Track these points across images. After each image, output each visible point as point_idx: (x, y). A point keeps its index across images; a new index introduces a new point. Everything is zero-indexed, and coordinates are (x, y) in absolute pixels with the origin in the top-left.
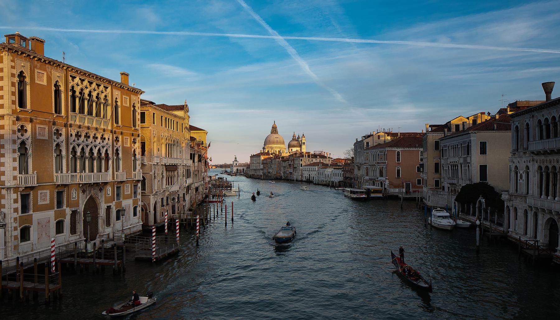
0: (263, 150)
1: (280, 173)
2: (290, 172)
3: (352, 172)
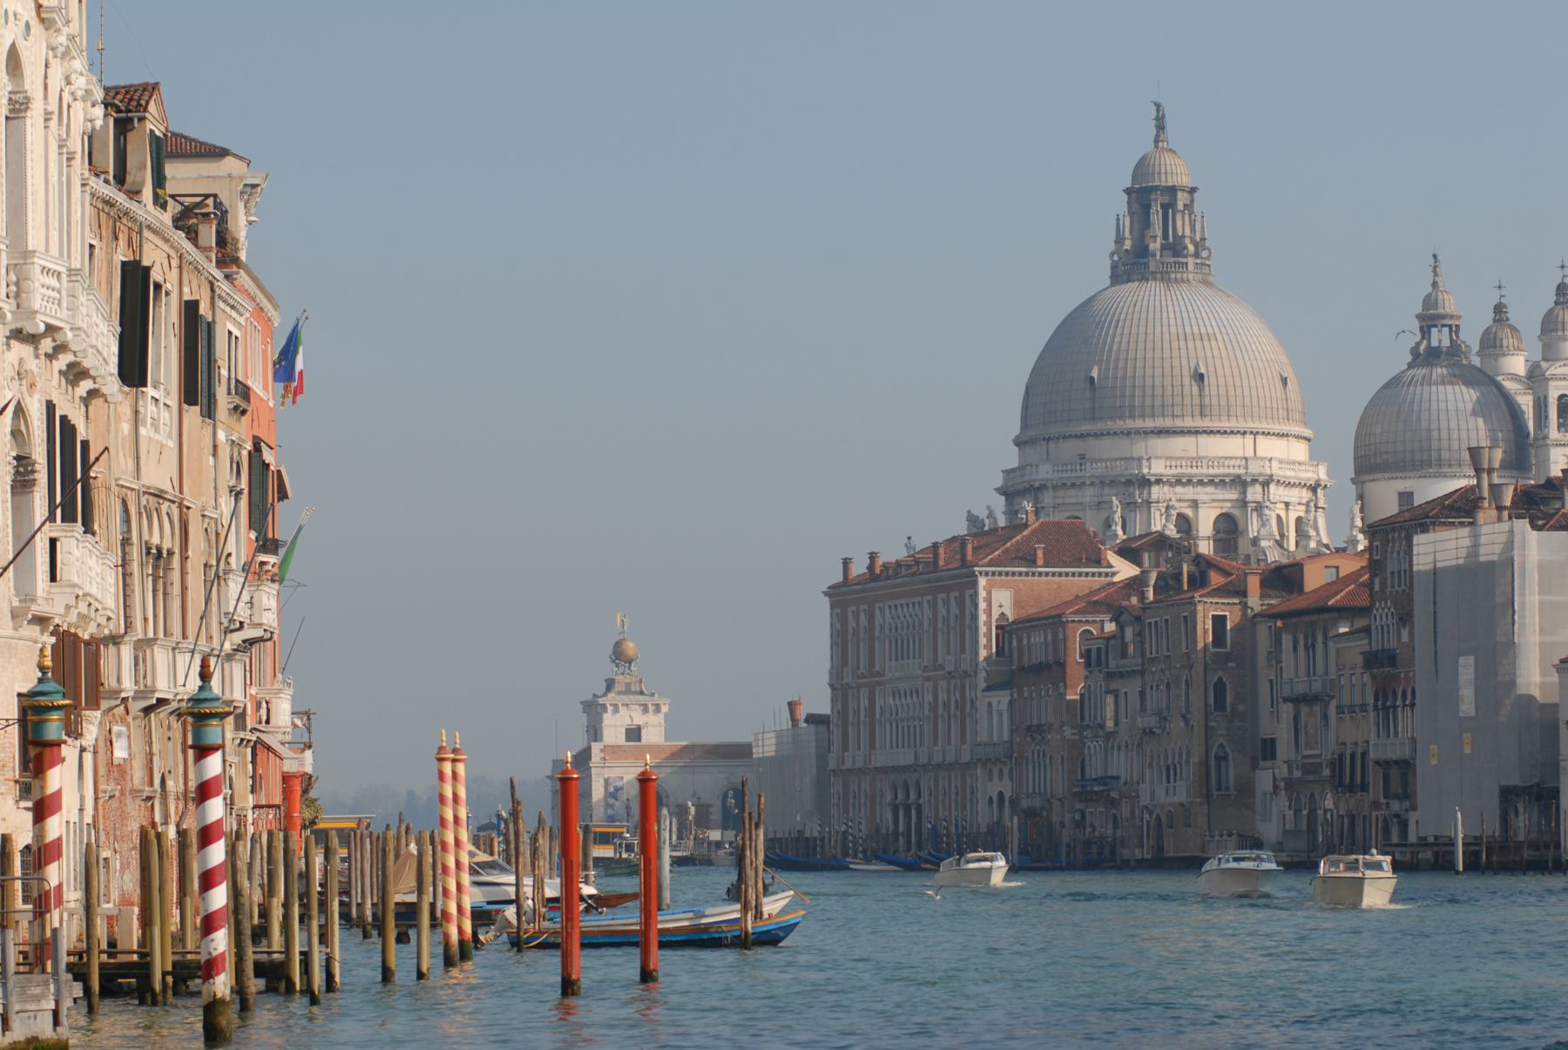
0: (1012, 512)
1: (1246, 790)
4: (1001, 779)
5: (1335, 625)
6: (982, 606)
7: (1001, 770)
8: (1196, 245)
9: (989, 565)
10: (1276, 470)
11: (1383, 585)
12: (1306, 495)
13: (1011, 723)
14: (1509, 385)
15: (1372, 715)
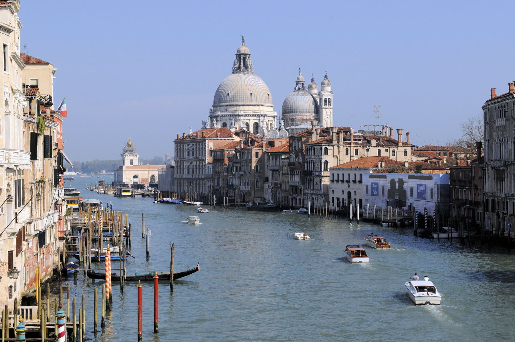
0: (212, 121)
1: (262, 188)
2: (292, 186)
3: (476, 187)
4: (210, 182)
5: (281, 156)
6: (207, 146)
7: (210, 180)
8: (250, 66)
9: (208, 137)
10: (266, 113)
11: (292, 149)
12: (272, 118)
13: (213, 171)
14: (314, 95)
15: (289, 176)
